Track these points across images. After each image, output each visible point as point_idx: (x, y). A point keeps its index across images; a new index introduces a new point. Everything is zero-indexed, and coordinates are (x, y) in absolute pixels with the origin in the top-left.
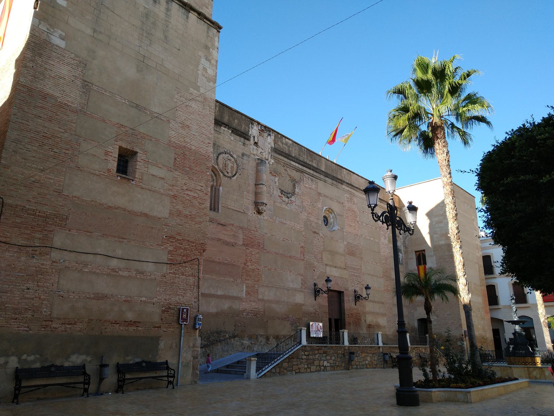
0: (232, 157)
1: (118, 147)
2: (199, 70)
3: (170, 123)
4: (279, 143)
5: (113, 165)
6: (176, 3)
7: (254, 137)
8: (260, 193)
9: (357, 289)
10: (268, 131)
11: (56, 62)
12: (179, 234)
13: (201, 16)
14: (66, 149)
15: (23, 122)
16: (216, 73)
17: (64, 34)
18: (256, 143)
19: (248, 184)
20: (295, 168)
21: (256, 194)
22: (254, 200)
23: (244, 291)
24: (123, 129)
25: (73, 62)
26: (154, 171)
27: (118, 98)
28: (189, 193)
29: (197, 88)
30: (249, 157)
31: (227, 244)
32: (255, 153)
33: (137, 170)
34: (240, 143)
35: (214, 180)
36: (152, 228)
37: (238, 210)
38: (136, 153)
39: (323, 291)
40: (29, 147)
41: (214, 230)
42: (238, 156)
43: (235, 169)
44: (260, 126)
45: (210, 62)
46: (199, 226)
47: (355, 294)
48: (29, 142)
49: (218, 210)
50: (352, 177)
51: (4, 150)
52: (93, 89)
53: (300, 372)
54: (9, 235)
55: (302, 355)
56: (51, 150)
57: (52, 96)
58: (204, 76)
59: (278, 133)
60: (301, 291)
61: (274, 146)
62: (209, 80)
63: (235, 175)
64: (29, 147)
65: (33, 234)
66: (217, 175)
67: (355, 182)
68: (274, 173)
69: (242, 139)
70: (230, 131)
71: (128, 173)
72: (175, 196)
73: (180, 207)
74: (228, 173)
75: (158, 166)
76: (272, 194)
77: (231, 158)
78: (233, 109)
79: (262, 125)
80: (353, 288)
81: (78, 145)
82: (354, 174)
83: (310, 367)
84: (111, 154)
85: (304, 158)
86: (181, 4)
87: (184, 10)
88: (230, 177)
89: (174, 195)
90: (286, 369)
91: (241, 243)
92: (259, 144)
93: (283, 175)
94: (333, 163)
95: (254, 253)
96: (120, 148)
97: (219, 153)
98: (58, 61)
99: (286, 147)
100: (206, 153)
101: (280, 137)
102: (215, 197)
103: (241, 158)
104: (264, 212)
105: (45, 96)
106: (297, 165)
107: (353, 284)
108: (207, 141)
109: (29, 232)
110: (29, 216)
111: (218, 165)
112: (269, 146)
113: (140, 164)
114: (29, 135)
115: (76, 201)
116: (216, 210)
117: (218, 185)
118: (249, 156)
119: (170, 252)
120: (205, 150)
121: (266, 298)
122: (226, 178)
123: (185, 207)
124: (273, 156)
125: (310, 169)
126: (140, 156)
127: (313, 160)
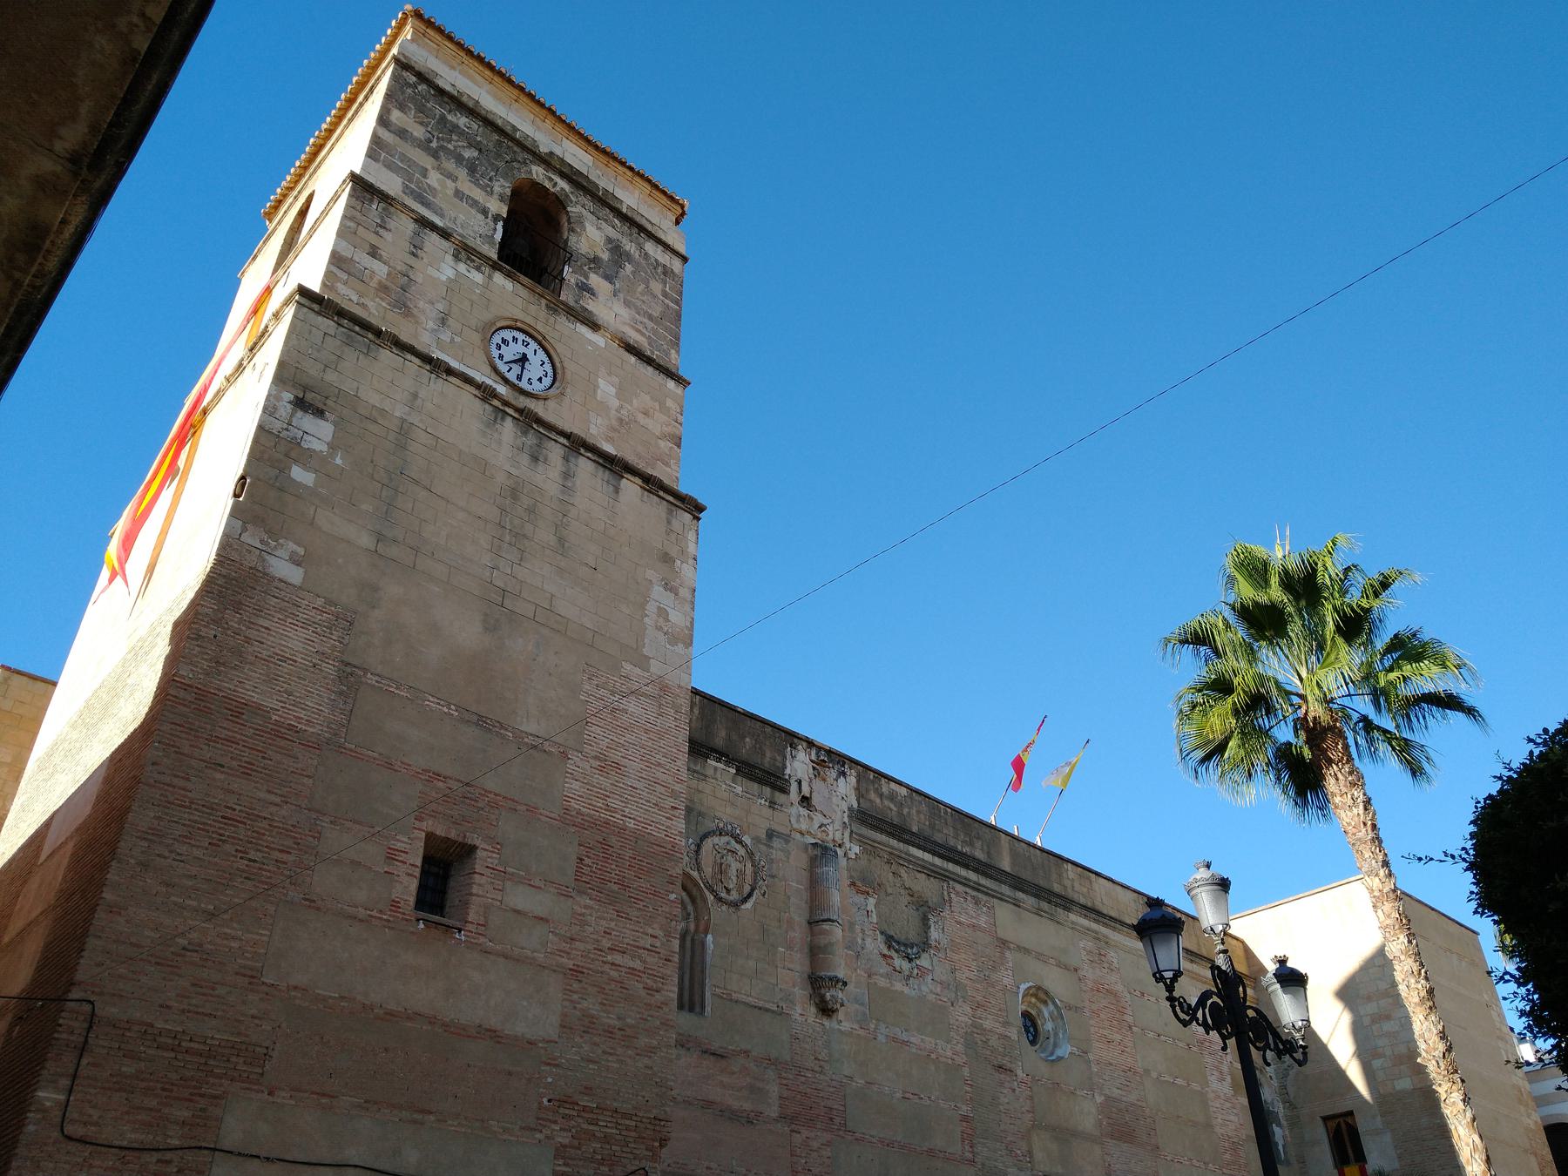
0: (740, 842)
1: (424, 834)
2: (647, 615)
3: (569, 759)
4: (872, 796)
5: (407, 887)
6: (588, 458)
7: (800, 783)
8: (826, 946)
10: (838, 763)
11: (277, 620)
12: (588, 1090)
13: (652, 484)
14: (281, 851)
15: (176, 781)
16: (693, 619)
17: (301, 551)
18: (805, 801)
19: (788, 921)
20: (924, 867)
21: (816, 952)
22: (807, 969)
24: (441, 784)
25: (319, 617)
26: (520, 898)
27: (431, 703)
28: (618, 958)
29: (643, 662)
30: (787, 842)
31: (733, 1116)
32: (804, 827)
33: (474, 898)
34: (759, 801)
35: (689, 914)
36: (510, 1074)
37: (761, 1004)
38: (473, 848)
40: (183, 849)
41: (689, 1073)
42: (756, 840)
43: (749, 879)
44: (814, 752)
45: (676, 594)
46: (646, 1061)
48: (186, 837)
49: (703, 1007)
50: (1096, 886)
51: (113, 863)
52: (367, 683)
54: (95, 1114)
56: (241, 855)
57: (258, 709)
58: (659, 628)
59: (867, 768)
61: (859, 803)
62: (674, 639)
63: (750, 895)
64: (183, 849)
65: (166, 1110)
66: (698, 901)
67: (1105, 902)
68: (863, 884)
69: (767, 790)
70: (730, 769)
71: (447, 910)
72: (576, 972)
73: (591, 1005)
74: (728, 891)
75: (532, 883)
76: (859, 949)
77: (738, 847)
78: (739, 710)
79: (820, 748)
81: (314, 838)
82: (1100, 879)
84: (403, 857)
86: (601, 461)
87: (607, 472)
88: (735, 905)
89: (575, 968)
91: (773, 1111)
92: (815, 801)
93: (890, 890)
94: (1035, 846)
95: (815, 1145)
96: (430, 837)
98: (281, 617)
99: (892, 806)
100: (666, 835)
101: (871, 777)
102: (692, 969)
103: (765, 844)
104: (839, 1006)
105: (239, 710)
106: (927, 857)
108: (670, 802)
109: (154, 1103)
110: (160, 1052)
111: (699, 870)
112: (845, 806)
113: (483, 880)
114: (186, 816)
115: (297, 1002)
116: (698, 1009)
117: (702, 928)
118: (787, 839)
119: (560, 1152)
120: (664, 828)
122: (724, 907)
123: (605, 1005)
124: (856, 834)
125: (966, 866)
126: (485, 858)
127: (975, 840)
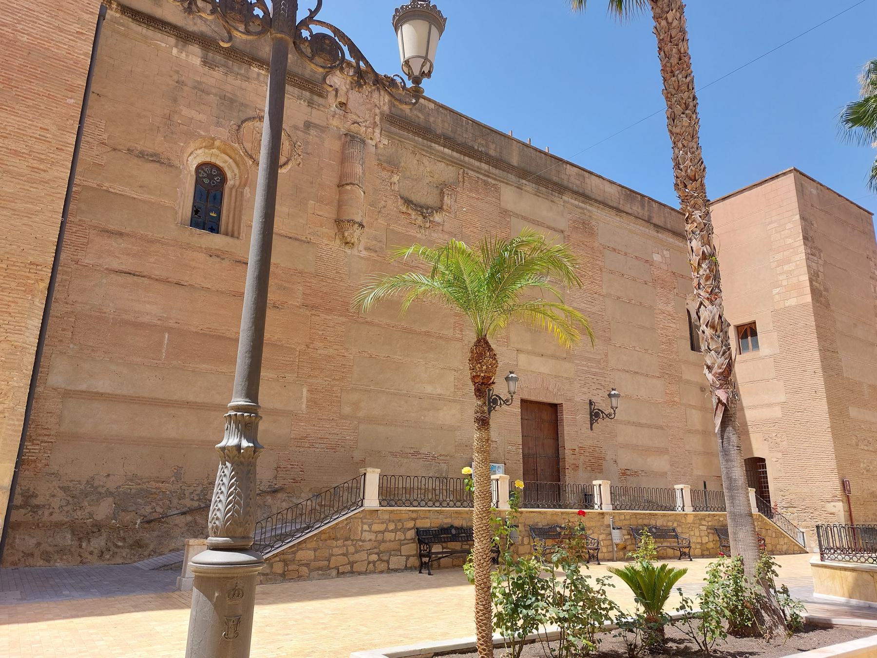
9: (594, 399)
23: (304, 400)
35: (235, 175)
39: (502, 400)
42: (296, 128)
46: (25, 221)
47: (590, 409)
49: (239, 234)
50: (587, 181)
53: (352, 572)
55: (362, 531)
60: (454, 401)
67: (593, 191)
69: (307, 94)
80: (586, 398)
82: (593, 176)
83: (385, 558)
85: (466, 136)
90: (307, 565)
92: (350, 105)
94: (541, 152)
97: (243, 118)
99: (420, 115)
100: (67, 53)
103: (302, 131)
107: (585, 390)
120: (66, 47)
121: (361, 414)
124: (384, 131)
125: (480, 160)
